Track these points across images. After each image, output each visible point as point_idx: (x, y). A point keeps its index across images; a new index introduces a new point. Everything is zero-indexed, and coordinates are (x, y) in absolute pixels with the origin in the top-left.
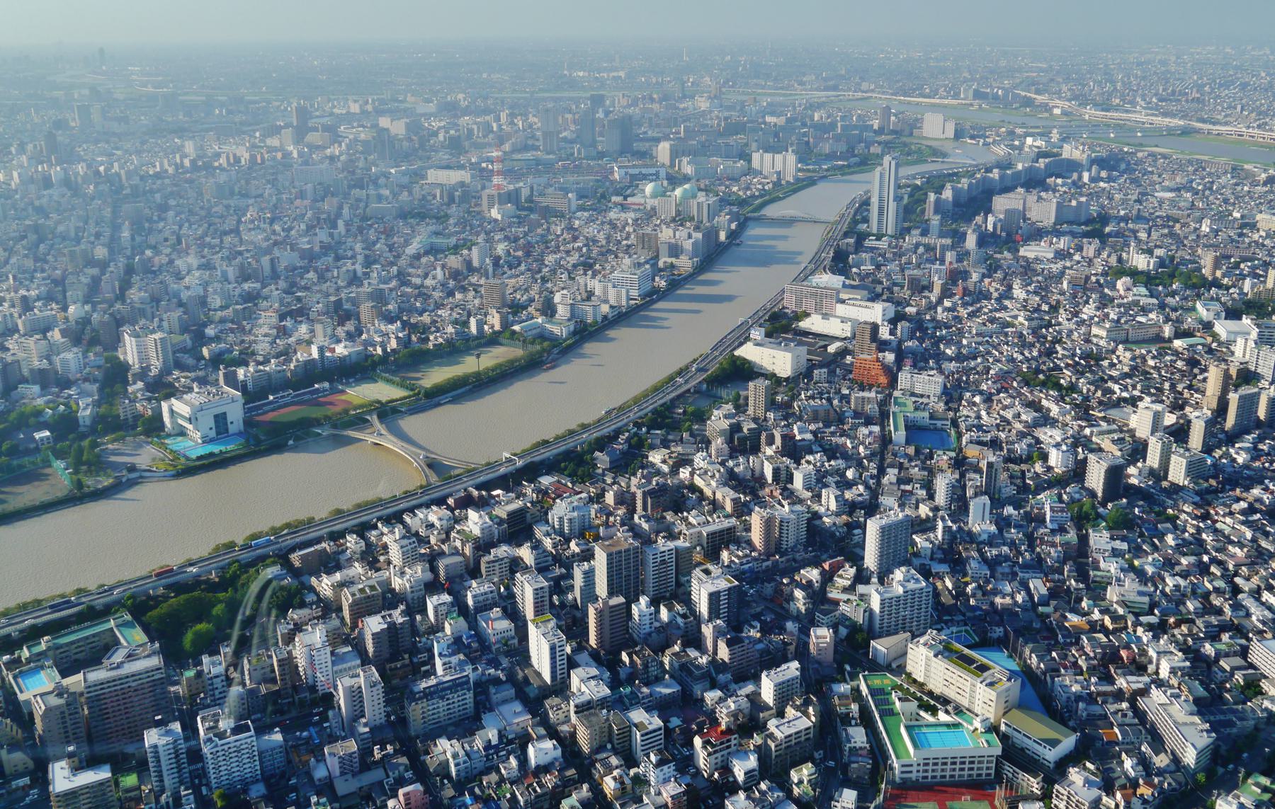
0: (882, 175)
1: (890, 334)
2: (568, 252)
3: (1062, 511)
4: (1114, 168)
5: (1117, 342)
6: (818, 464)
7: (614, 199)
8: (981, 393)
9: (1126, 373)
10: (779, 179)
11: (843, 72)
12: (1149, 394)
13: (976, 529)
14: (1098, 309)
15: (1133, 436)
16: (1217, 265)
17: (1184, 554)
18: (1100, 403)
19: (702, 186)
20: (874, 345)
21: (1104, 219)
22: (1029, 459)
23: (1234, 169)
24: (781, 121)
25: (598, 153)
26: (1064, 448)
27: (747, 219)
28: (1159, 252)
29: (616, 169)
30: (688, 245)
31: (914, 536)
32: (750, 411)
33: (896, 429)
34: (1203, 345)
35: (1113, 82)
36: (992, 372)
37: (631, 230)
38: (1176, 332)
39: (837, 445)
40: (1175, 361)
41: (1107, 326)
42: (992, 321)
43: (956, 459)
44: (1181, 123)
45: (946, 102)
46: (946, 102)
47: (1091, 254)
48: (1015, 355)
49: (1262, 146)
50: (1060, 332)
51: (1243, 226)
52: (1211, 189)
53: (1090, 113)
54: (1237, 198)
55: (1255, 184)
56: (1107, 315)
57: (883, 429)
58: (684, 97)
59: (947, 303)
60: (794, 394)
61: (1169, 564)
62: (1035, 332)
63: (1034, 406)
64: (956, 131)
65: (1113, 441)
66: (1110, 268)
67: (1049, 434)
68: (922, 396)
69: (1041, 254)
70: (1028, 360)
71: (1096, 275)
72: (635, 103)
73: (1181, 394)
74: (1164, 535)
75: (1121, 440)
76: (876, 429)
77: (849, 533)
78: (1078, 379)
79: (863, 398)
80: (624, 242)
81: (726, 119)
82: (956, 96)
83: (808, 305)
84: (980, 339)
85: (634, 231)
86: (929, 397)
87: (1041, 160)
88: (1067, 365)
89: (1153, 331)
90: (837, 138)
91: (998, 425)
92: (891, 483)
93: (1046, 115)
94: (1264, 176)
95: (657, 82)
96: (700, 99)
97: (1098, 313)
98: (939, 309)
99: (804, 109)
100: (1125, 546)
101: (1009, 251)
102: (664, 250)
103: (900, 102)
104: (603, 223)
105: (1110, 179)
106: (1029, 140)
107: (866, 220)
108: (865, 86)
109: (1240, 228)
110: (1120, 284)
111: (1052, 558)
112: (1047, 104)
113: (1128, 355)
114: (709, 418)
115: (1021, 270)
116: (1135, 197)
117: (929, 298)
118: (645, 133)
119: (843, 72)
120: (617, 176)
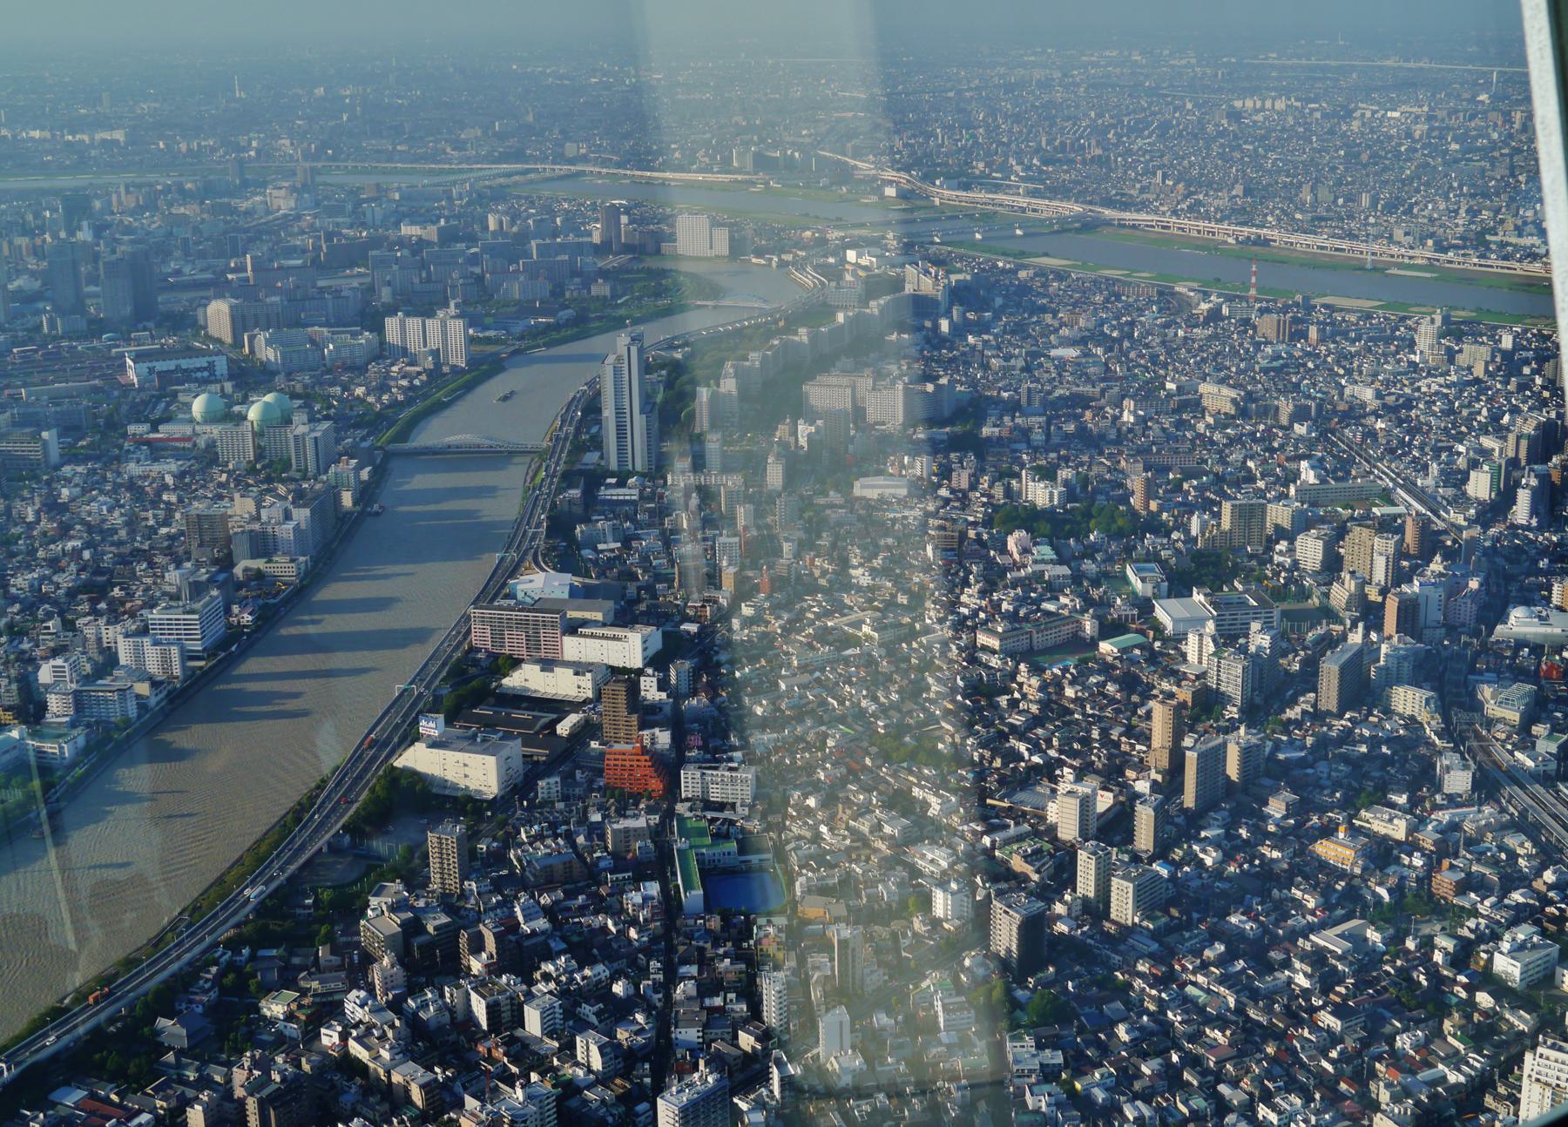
0: (617, 372)
1: (659, 689)
2: (54, 564)
3: (961, 1009)
4: (983, 305)
5: (1016, 655)
6: (563, 978)
7: (132, 429)
8: (816, 787)
9: (1035, 717)
10: (438, 364)
11: (530, 118)
12: (1074, 754)
13: (833, 1065)
14: (983, 594)
15: (1054, 839)
16: (1149, 494)
17: (1145, 1056)
18: (1002, 781)
19: (299, 388)
20: (634, 717)
21: (975, 408)
22: (900, 911)
23: (1160, 293)
24: (431, 233)
25: (91, 322)
26: (954, 886)
27: (389, 456)
28: (1065, 473)
29: (129, 362)
30: (286, 531)
31: (736, 1100)
32: (435, 886)
33: (688, 886)
34: (1140, 646)
35: (969, 126)
36: (830, 743)
37: (174, 499)
38: (1101, 624)
39: (592, 930)
40: (1104, 685)
41: (1000, 630)
42: (824, 635)
43: (788, 929)
44: (1078, 208)
45: (710, 177)
46: (710, 177)
47: (965, 484)
48: (864, 703)
49: (1197, 247)
50: (929, 648)
51: (1183, 407)
52: (1130, 336)
53: (943, 194)
54: (1168, 353)
55: (1192, 322)
56: (997, 606)
57: (664, 890)
58: (245, 184)
59: (747, 611)
60: (507, 833)
61: (1125, 1079)
62: (890, 649)
63: (900, 802)
64: (732, 239)
65: (1026, 858)
66: (996, 508)
67: (930, 856)
68: (721, 807)
69: (888, 491)
70: (884, 710)
71: (975, 524)
72: (150, 205)
73: (1117, 745)
74: (1114, 1023)
75: (1037, 852)
76: (653, 888)
77: (631, 1115)
78: (964, 739)
79: (627, 830)
80: (164, 531)
81: (329, 236)
82: (726, 167)
83: (514, 643)
84: (806, 678)
85: (180, 500)
86: (733, 806)
87: (873, 303)
88: (947, 712)
89: (1067, 629)
90: (533, 272)
91: (849, 850)
92: (689, 998)
93: (874, 199)
94: (1204, 306)
95: (189, 150)
96: (275, 193)
97: (984, 603)
98: (736, 624)
99: (468, 204)
100: (1058, 1058)
101: (838, 491)
102: (240, 547)
103: (636, 182)
104: (117, 487)
105: (981, 328)
106: (851, 255)
107: (597, 443)
108: (570, 149)
109: (1174, 412)
110: (1011, 543)
111: (953, 1102)
112: (875, 178)
113: (1035, 682)
114: (363, 914)
115: (860, 525)
116: (1020, 363)
117: (716, 602)
118: (178, 272)
119: (530, 118)
120: (132, 376)
